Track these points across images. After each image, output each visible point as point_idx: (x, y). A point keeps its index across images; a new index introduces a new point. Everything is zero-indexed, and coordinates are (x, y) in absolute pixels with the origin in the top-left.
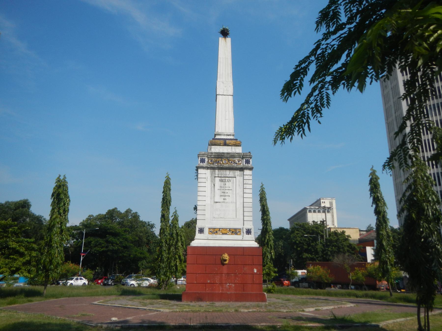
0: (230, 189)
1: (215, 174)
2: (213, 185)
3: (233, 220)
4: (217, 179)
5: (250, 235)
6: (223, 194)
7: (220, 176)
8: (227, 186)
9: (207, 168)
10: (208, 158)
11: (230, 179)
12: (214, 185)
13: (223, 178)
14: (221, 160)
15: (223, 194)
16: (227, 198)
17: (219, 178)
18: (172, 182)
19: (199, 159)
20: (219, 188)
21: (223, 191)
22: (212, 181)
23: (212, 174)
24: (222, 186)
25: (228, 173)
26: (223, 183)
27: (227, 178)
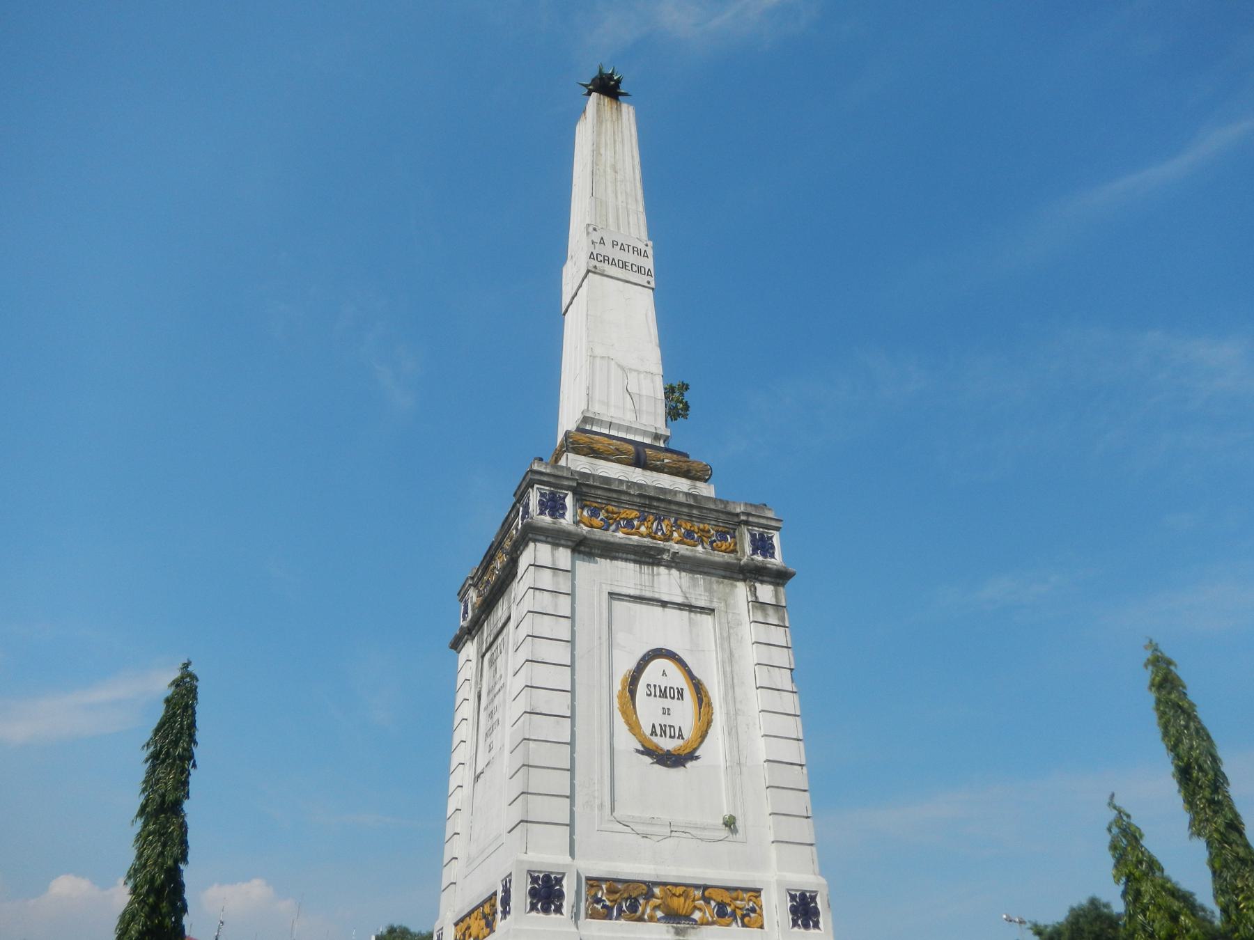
5: (553, 916)
10: (475, 586)
18: (1182, 671)
22: (476, 683)
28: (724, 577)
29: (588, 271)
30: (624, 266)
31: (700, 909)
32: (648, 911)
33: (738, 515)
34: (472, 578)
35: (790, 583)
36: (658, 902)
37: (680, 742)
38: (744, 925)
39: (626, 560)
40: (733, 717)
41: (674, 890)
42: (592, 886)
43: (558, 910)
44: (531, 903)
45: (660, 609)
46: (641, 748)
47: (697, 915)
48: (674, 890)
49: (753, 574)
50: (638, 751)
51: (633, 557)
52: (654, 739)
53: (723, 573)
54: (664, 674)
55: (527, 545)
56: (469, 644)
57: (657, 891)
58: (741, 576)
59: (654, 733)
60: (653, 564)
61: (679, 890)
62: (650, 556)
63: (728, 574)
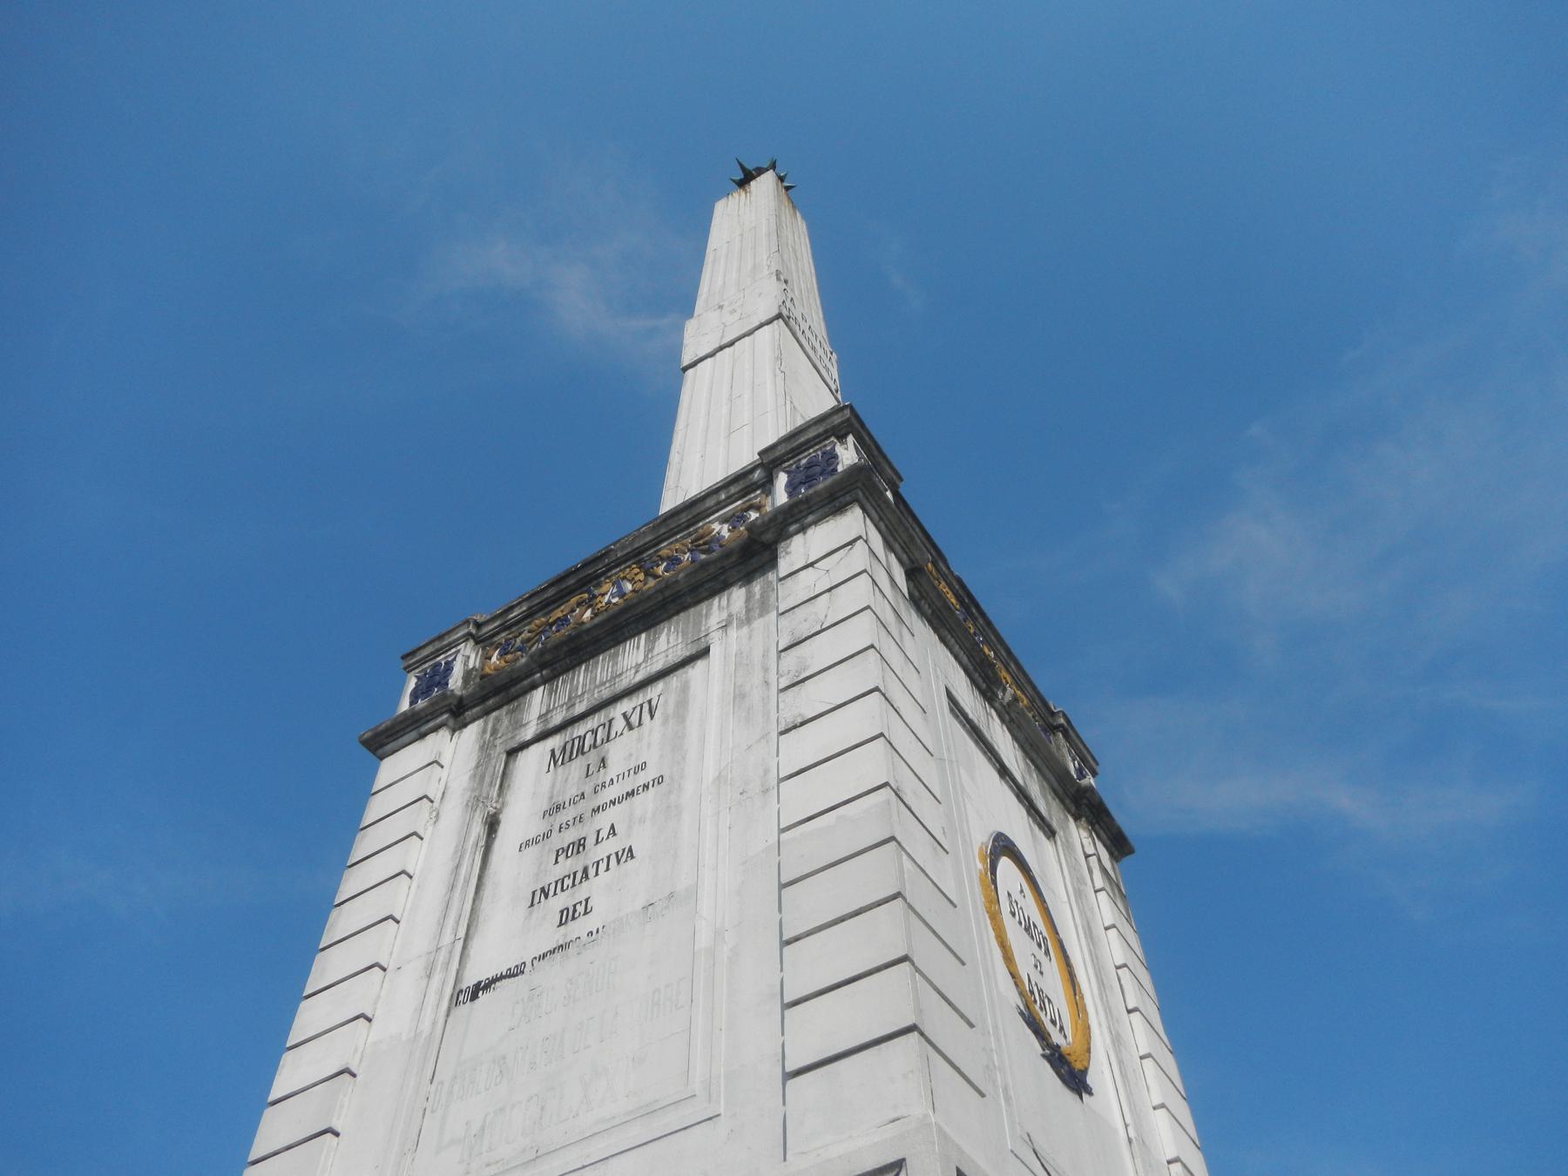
0: (643, 778)
1: (519, 725)
2: (478, 829)
3: (637, 1133)
4: (533, 760)
6: (567, 865)
7: (557, 719)
8: (616, 766)
9: (458, 713)
11: (653, 692)
12: (492, 825)
13: (580, 729)
14: (589, 603)
15: (567, 865)
16: (596, 888)
17: (555, 742)
19: (412, 683)
20: (536, 828)
21: (571, 836)
22: (476, 801)
23: (485, 748)
24: (573, 791)
25: (633, 658)
26: (577, 767)
27: (625, 706)
28: (1055, 791)
29: (779, 316)
30: (813, 348)
33: (1053, 714)
34: (478, 626)
35: (1127, 860)
39: (956, 657)
40: (1117, 1040)
45: (996, 776)
49: (1089, 808)
50: (1021, 1014)
51: (965, 660)
53: (1056, 785)
55: (840, 510)
56: (444, 734)
58: (1073, 809)
60: (983, 693)
62: (986, 678)
63: (1061, 792)
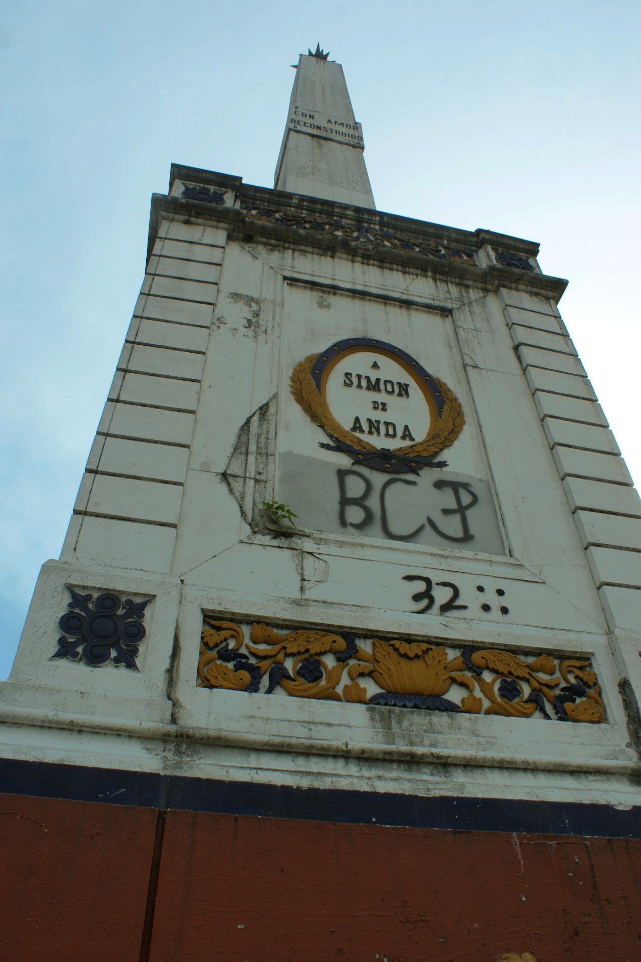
31: (462, 685)
32: (345, 680)
36: (367, 666)
37: (408, 443)
38: (563, 716)
41: (404, 647)
42: (219, 629)
43: (128, 659)
44: (62, 642)
46: (327, 440)
47: (455, 695)
48: (404, 647)
52: (357, 434)
54: (375, 366)
57: (365, 646)
59: (357, 425)
61: (413, 649)
